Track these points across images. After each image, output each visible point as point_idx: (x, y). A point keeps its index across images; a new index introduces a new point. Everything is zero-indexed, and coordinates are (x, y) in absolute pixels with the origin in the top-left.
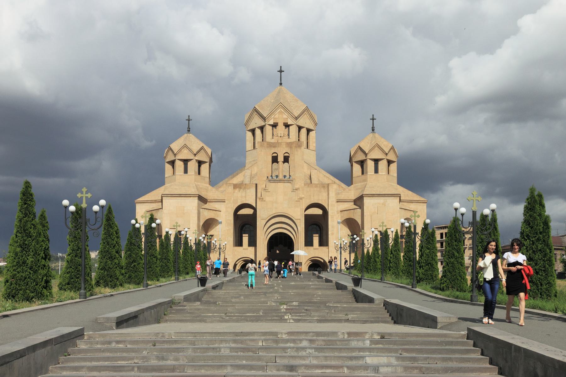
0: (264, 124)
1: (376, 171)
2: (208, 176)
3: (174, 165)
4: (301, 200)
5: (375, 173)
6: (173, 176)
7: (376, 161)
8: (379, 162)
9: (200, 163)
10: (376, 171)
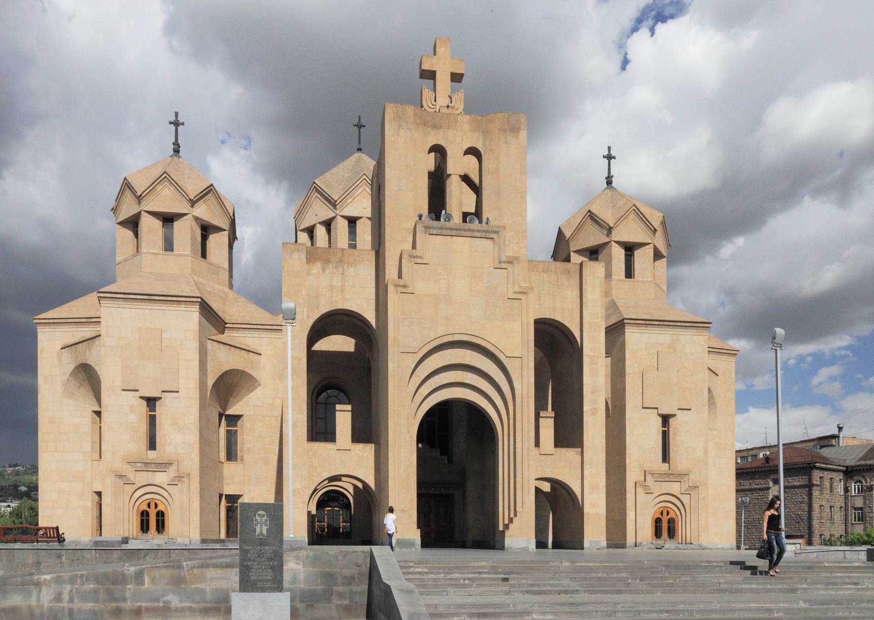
0: (335, 215)
1: (629, 273)
2: (226, 265)
3: (137, 231)
4: (524, 296)
5: (626, 277)
6: (134, 256)
7: (630, 249)
8: (635, 252)
9: (206, 230)
10: (629, 273)
